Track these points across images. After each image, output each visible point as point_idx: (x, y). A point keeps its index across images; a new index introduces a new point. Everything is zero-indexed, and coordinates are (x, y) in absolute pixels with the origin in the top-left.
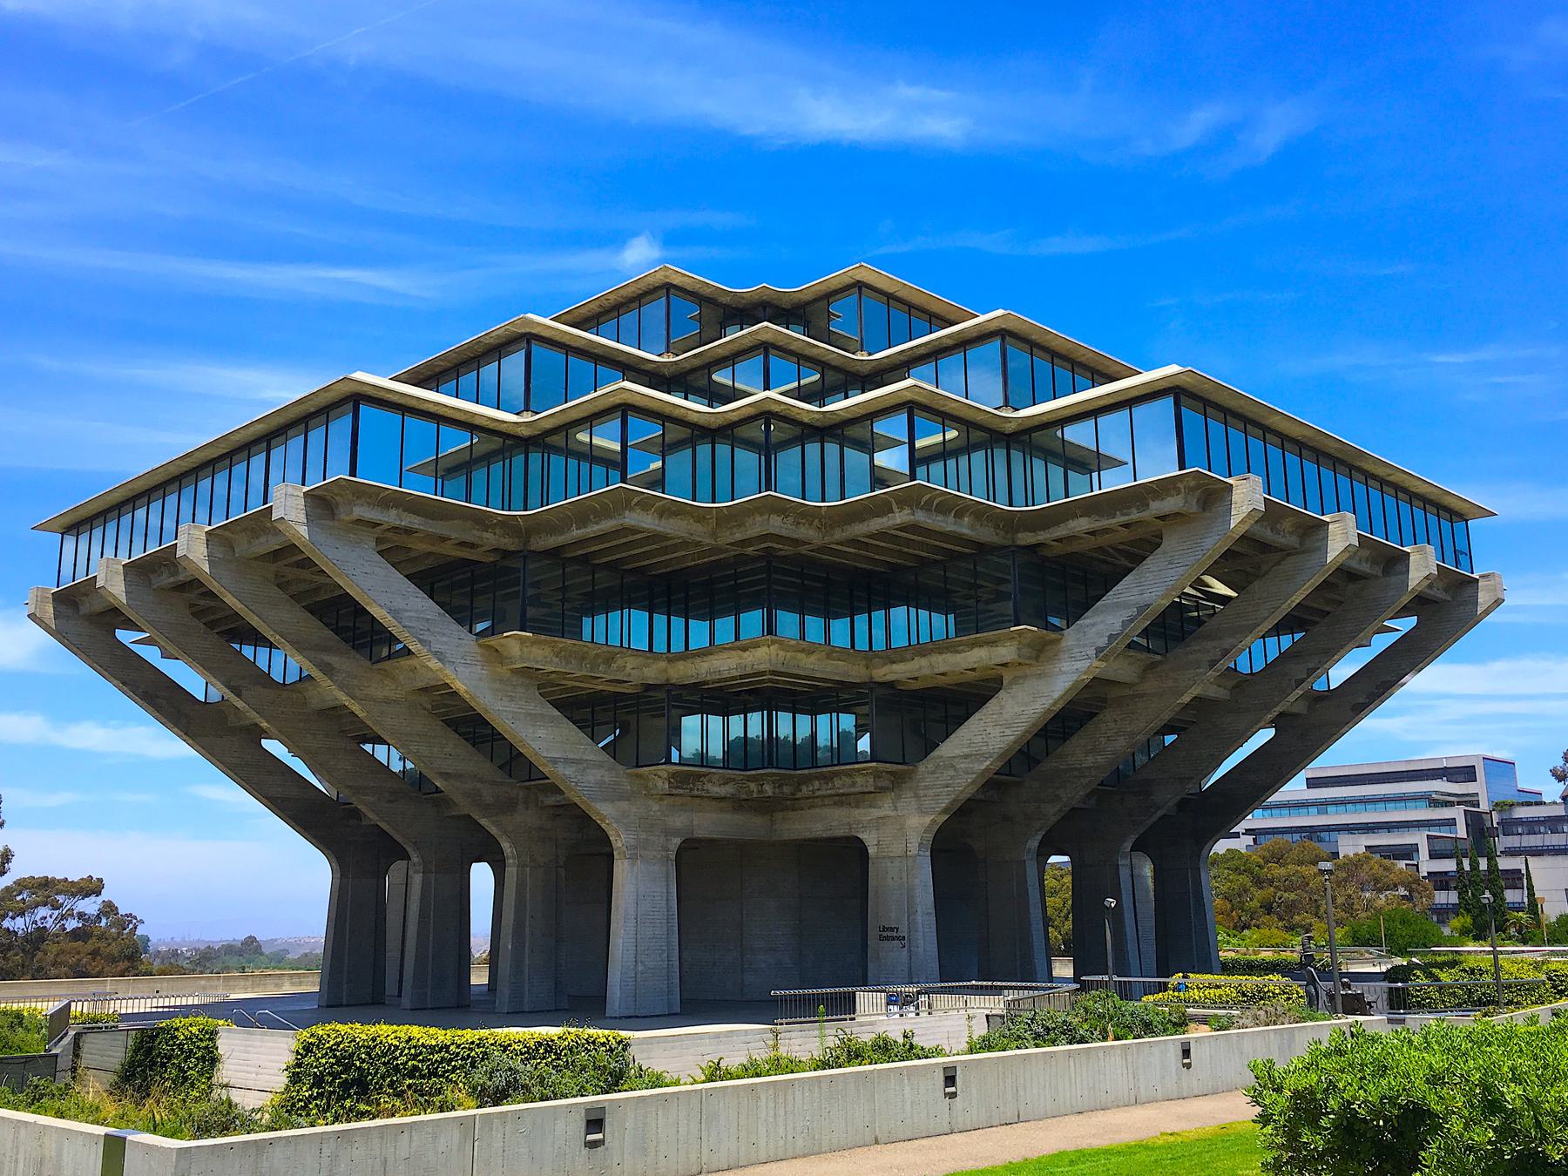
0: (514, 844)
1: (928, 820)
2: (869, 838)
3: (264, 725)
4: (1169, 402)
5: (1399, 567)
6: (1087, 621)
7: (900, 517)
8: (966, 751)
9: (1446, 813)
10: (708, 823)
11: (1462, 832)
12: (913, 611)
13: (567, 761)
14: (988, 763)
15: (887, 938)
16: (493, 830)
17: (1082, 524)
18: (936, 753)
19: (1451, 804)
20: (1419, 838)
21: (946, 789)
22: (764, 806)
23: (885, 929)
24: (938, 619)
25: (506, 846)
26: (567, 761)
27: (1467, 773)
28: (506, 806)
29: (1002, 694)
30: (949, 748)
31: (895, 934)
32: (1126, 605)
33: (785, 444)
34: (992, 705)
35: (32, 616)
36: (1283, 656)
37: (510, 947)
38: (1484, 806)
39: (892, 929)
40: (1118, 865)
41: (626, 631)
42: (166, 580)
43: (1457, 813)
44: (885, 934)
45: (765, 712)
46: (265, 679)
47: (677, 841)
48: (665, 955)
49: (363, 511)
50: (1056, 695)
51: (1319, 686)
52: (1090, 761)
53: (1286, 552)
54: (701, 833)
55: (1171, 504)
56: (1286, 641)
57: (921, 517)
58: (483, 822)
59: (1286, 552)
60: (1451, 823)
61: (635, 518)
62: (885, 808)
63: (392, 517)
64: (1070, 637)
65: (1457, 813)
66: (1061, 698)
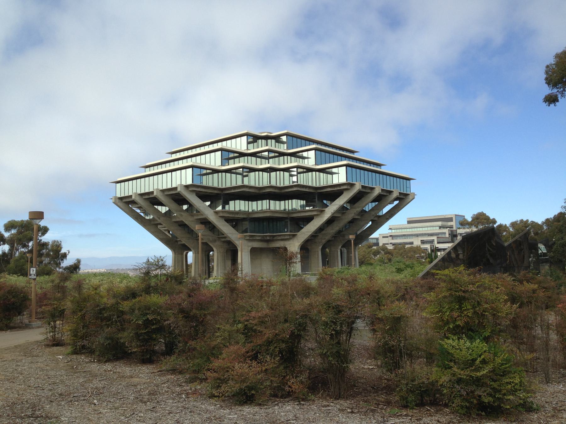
0: (216, 248)
1: (300, 244)
5: (392, 194)
8: (307, 231)
10: (256, 245)
11: (447, 236)
12: (297, 209)
13: (230, 233)
16: (212, 246)
17: (329, 189)
19: (446, 228)
20: (435, 238)
22: (268, 241)
24: (302, 201)
26: (230, 233)
27: (450, 220)
28: (215, 241)
29: (314, 220)
32: (337, 205)
34: (312, 222)
35: (114, 203)
38: (454, 228)
42: (147, 197)
43: (446, 231)
47: (250, 248)
51: (380, 214)
52: (331, 231)
53: (369, 193)
54: (254, 246)
55: (345, 187)
56: (374, 204)
57: (299, 189)
58: (210, 244)
59: (369, 193)
60: (445, 233)
62: (291, 242)
64: (327, 209)
65: (446, 231)
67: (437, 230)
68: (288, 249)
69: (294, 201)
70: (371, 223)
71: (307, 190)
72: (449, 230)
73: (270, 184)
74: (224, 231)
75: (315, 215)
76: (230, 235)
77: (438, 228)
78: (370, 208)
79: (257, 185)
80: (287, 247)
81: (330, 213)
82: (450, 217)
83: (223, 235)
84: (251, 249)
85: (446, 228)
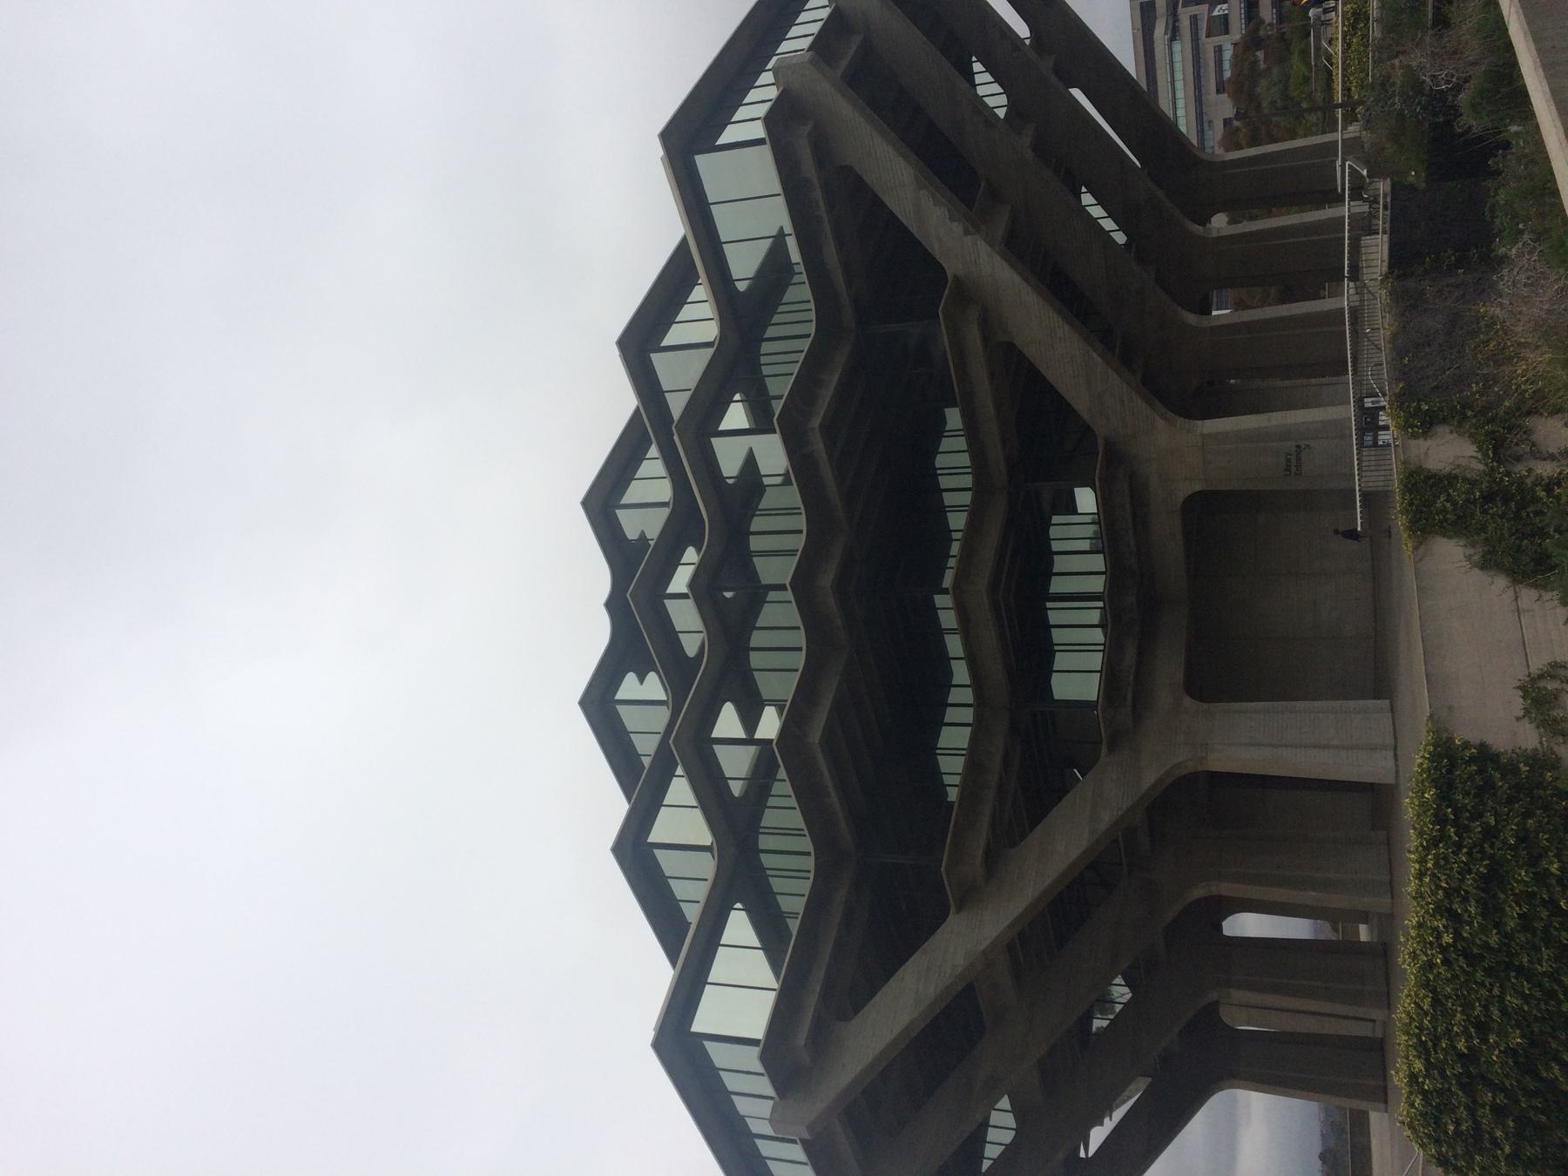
1: (1160, 422)
2: (1184, 490)
3: (1061, 1156)
4: (703, 162)
6: (936, 246)
7: (818, 446)
9: (1185, 23)
10: (1169, 669)
14: (1095, 355)
15: (1298, 466)
17: (831, 253)
18: (1086, 416)
20: (1208, 45)
21: (1126, 403)
23: (1288, 469)
25: (1199, 892)
30: (1080, 400)
31: (1293, 458)
33: (753, 575)
34: (1032, 353)
36: (989, 69)
37: (1314, 894)
39: (1289, 461)
40: (1218, 238)
41: (953, 752)
44: (1293, 469)
45: (1049, 605)
46: (1011, 1150)
47: (1188, 702)
48: (1321, 715)
49: (801, 1037)
50: (1017, 279)
54: (1180, 676)
57: (816, 422)
60: (1194, 20)
61: (816, 733)
63: (811, 1001)
64: (952, 267)
66: (1020, 274)
67: (1181, 50)
68: (1198, 487)
69: (941, 461)
70: (1077, 93)
71: (833, 379)
72: (1183, 7)
73: (782, 587)
74: (1074, 854)
75: (986, 339)
76: (1106, 818)
77: (1177, 47)
78: (996, 88)
79: (799, 660)
80: (1182, 500)
81: (968, 239)
82: (1138, 12)
83: (1116, 841)
84: (1191, 695)
85: (1178, 21)
